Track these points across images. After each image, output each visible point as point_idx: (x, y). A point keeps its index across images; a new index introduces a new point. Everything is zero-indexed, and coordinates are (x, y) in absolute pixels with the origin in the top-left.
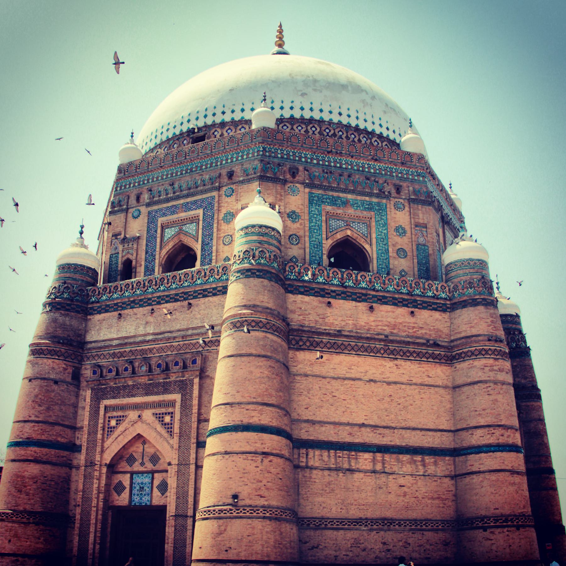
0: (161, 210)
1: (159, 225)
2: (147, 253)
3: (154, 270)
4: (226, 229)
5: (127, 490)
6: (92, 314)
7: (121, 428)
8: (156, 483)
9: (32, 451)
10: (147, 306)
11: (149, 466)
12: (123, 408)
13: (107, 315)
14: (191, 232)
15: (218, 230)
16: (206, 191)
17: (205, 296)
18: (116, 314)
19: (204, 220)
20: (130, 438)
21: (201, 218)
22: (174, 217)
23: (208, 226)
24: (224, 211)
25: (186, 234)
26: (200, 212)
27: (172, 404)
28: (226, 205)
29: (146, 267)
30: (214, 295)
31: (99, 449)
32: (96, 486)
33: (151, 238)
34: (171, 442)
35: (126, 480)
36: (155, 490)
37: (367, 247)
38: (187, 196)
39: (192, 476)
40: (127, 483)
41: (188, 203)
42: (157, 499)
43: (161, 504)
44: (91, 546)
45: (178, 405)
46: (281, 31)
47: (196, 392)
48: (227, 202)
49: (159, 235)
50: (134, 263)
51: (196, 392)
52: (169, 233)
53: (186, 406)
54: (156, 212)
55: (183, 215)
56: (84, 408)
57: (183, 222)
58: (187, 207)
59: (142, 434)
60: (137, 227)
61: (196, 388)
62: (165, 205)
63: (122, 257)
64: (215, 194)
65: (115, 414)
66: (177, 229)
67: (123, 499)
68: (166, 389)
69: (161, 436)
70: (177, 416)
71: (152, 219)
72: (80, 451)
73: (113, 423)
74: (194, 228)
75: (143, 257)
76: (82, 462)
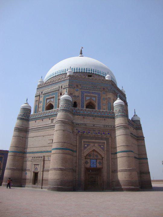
0: (85, 91)
1: (85, 95)
3: (84, 107)
5: (89, 163)
6: (74, 115)
7: (89, 147)
8: (98, 162)
9: (67, 151)
11: (96, 158)
12: (89, 142)
13: (80, 116)
15: (102, 101)
16: (98, 91)
21: (97, 97)
22: (89, 94)
23: (99, 100)
24: (103, 97)
25: (93, 100)
26: (97, 95)
27: (104, 143)
29: (81, 105)
30: (111, 118)
33: (83, 98)
34: (104, 152)
35: (89, 161)
36: (97, 163)
38: (93, 91)
42: (99, 166)
43: (99, 167)
46: (81, 51)
49: (85, 98)
50: (77, 103)
51: (110, 141)
52: (88, 98)
53: (108, 144)
55: (92, 95)
58: (93, 93)
60: (77, 94)
61: (110, 140)
62: (86, 90)
63: (74, 100)
64: (100, 92)
65: (86, 143)
66: (90, 98)
67: (88, 166)
68: (102, 139)
69: (101, 151)
71: (82, 93)
72: (76, 152)
73: (86, 146)
75: (80, 102)
76: (77, 155)
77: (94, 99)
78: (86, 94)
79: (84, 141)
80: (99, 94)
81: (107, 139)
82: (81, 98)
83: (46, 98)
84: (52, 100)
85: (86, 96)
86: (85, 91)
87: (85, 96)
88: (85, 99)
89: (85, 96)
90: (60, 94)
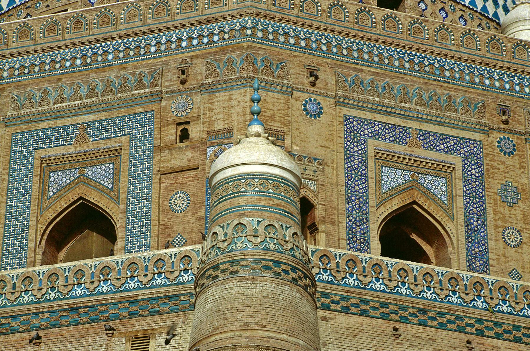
0: (372, 123)
1: (371, 152)
2: (349, 200)
4: (507, 212)
10: (456, 331)
14: (437, 193)
15: (496, 212)
18: (387, 326)
19: (466, 181)
22: (400, 149)
23: (476, 197)
25: (426, 192)
26: (457, 161)
28: (502, 167)
29: (350, 229)
33: (356, 174)
41: (428, 132)
48: (503, 163)
54: (361, 121)
57: (414, 165)
62: (379, 118)
64: (477, 136)
74: (444, 189)
75: (342, 206)
77: (438, 186)
78: (383, 145)
80: (473, 156)
82: (342, 177)
83: (39, 154)
84: (101, 173)
85: (385, 159)
86: (369, 116)
88: (372, 184)
89: (371, 163)
90: (171, 134)
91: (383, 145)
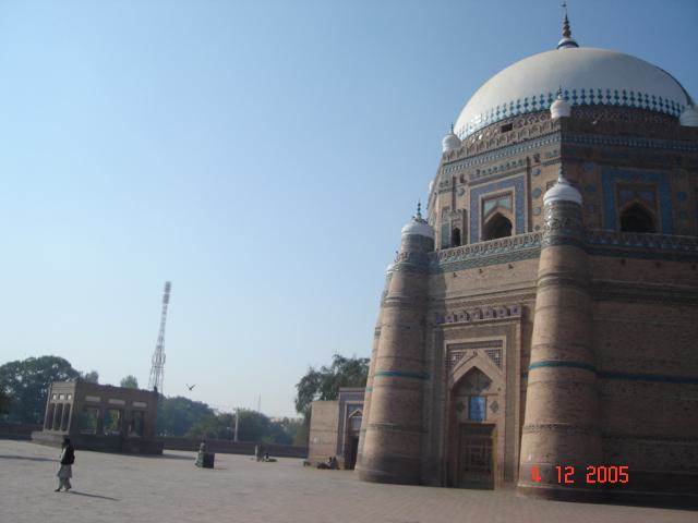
5: (467, 409)
7: (461, 362)
8: (489, 404)
17: (521, 259)
20: (467, 370)
25: (502, 207)
26: (513, 189)
27: (501, 341)
30: (529, 257)
31: (444, 378)
32: (443, 405)
35: (465, 401)
37: (654, 212)
39: (518, 400)
40: (466, 404)
44: (441, 451)
45: (504, 345)
46: (567, 22)
47: (518, 335)
50: (461, 232)
52: (489, 206)
55: (499, 192)
56: (430, 346)
58: (501, 185)
59: (479, 367)
60: (463, 203)
68: (495, 332)
70: (504, 353)
77: (505, 202)
79: (448, 346)
81: (509, 332)
85: (483, 201)
87: (480, 205)
91: (484, 195)
